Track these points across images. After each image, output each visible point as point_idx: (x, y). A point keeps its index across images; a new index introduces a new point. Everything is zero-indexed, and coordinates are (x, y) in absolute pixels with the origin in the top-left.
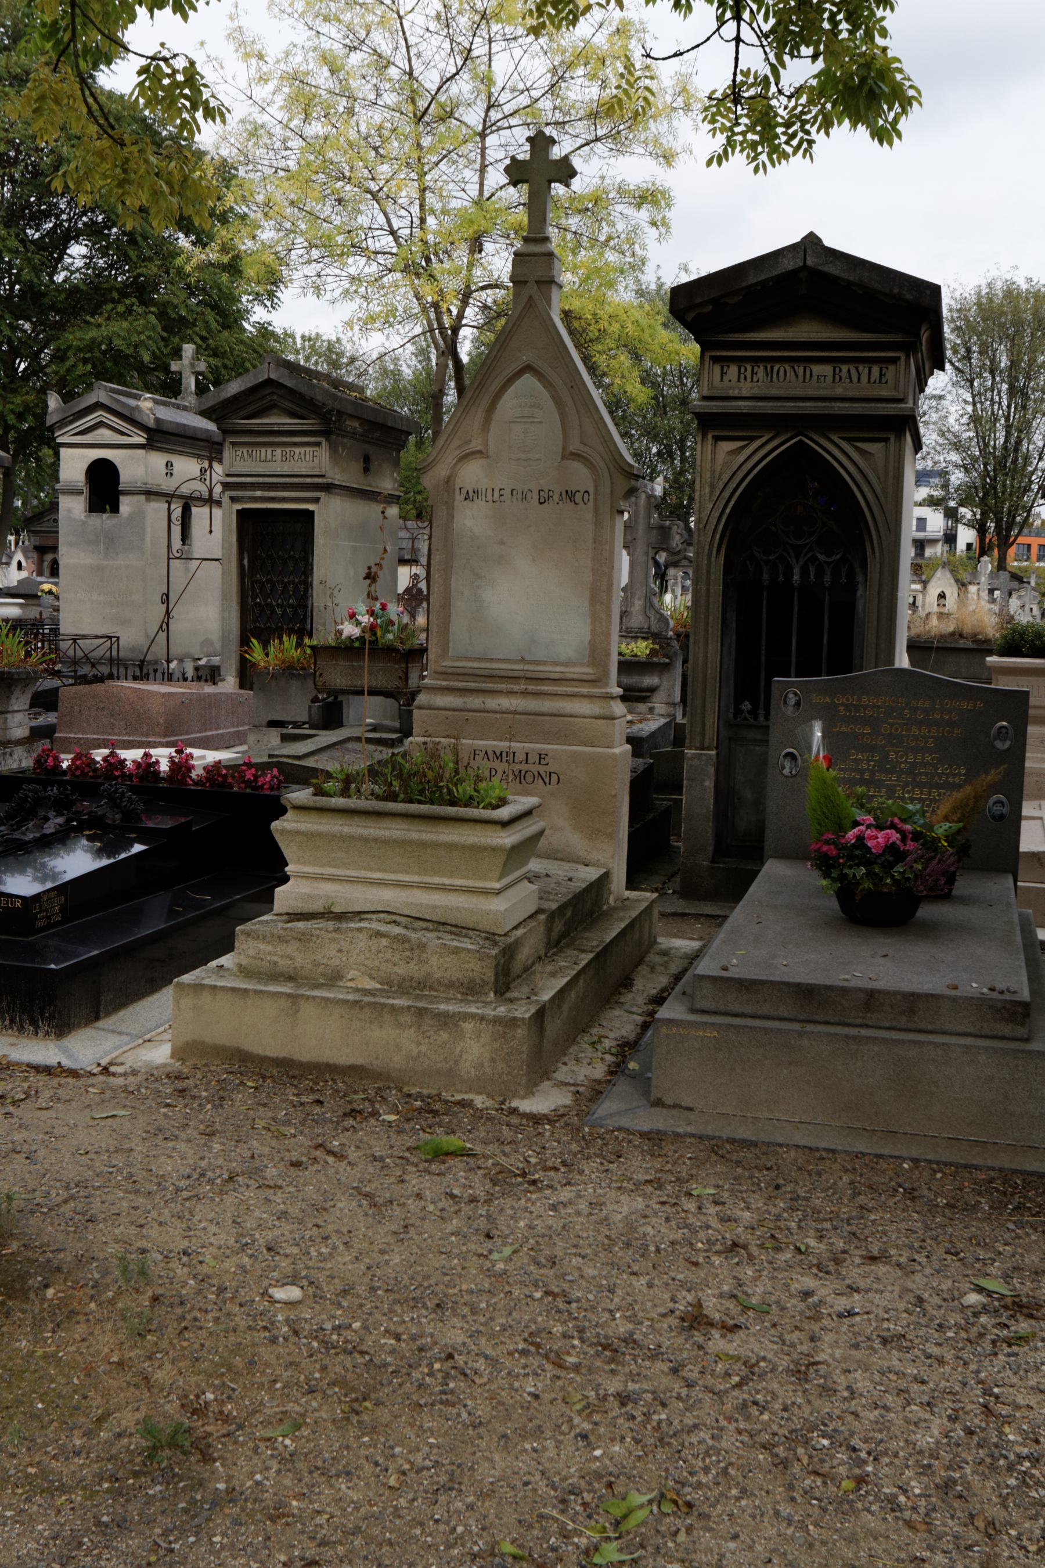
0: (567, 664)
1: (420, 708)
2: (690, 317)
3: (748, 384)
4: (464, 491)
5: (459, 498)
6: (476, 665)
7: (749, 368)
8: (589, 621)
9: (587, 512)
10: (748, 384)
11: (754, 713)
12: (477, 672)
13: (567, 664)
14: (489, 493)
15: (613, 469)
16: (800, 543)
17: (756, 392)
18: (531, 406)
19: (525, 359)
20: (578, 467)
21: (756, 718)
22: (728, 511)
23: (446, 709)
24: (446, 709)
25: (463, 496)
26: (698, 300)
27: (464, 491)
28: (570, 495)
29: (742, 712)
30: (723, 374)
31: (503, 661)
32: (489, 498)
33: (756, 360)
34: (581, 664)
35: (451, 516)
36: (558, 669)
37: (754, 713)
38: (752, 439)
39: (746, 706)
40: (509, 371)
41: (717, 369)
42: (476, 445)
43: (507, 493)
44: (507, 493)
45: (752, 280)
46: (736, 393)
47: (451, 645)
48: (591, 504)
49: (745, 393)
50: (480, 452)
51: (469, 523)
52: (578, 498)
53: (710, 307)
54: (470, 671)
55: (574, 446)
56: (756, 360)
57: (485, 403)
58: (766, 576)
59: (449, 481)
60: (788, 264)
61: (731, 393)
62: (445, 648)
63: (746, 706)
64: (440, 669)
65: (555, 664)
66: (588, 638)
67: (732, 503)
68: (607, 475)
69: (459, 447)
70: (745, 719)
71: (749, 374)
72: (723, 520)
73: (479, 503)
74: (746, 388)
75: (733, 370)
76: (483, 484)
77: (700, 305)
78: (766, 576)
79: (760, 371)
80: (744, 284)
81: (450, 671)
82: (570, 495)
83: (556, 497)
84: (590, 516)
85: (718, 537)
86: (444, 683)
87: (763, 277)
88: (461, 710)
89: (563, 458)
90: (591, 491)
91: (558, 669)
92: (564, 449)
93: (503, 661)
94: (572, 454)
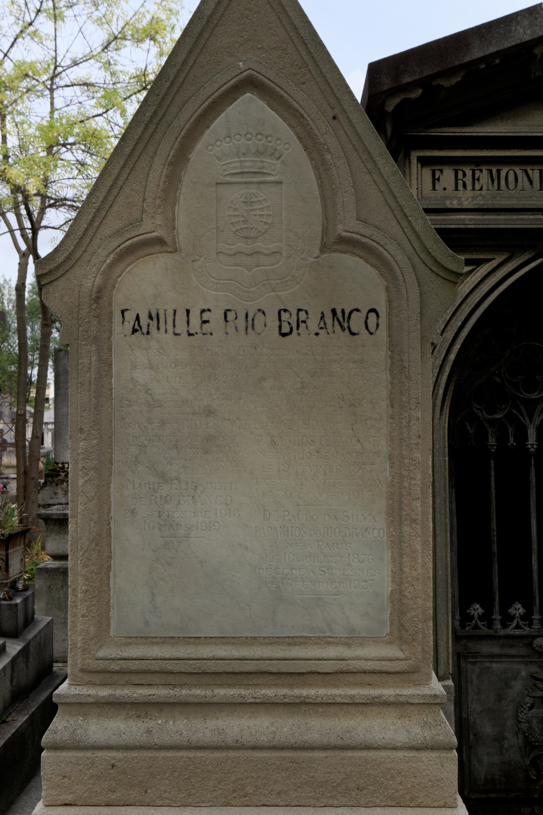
0: (351, 640)
1: (55, 747)
2: (508, 19)
3: (469, 193)
4: (130, 317)
5: (120, 330)
6: (166, 652)
7: (469, 173)
8: (387, 555)
9: (376, 348)
10: (469, 193)
11: (487, 618)
12: (170, 666)
13: (348, 642)
14: (181, 317)
15: (421, 267)
16: (533, 396)
17: (480, 203)
18: (259, 153)
19: (243, 65)
20: (351, 263)
21: (490, 625)
22: (452, 357)
23: (110, 748)
24: (110, 748)
25: (129, 326)
26: (407, 79)
27: (130, 317)
28: (341, 318)
29: (472, 617)
30: (435, 180)
31: (222, 640)
32: (181, 327)
33: (478, 162)
34: (377, 641)
35: (106, 365)
36: (332, 652)
37: (487, 618)
38: (478, 263)
39: (477, 610)
40: (212, 88)
41: (427, 173)
42: (152, 227)
43: (216, 317)
44: (216, 317)
45: (476, 53)
46: (455, 204)
47: (113, 614)
48: (382, 334)
49: (466, 204)
50: (160, 241)
51: (142, 376)
52: (357, 322)
53: (420, 91)
54: (155, 666)
55: (348, 225)
56: (478, 162)
57: (167, 148)
58: (492, 441)
59: (100, 296)
60: (523, 34)
61: (448, 204)
62: (103, 622)
63: (477, 610)
64: (95, 665)
65: (325, 641)
66: (388, 588)
67: (457, 346)
68: (411, 278)
69: (119, 232)
70: (476, 627)
71: (468, 180)
72: (447, 369)
73: (162, 337)
74: (467, 198)
75: (447, 176)
76: (170, 301)
77: (406, 88)
78: (492, 441)
79: (484, 176)
80: (467, 59)
81: (115, 666)
82: (341, 318)
83: (313, 323)
84: (381, 355)
85: (441, 391)
86: (104, 692)
87: (492, 49)
88: (141, 748)
89: (324, 248)
90: (382, 310)
91: (332, 652)
92: (325, 232)
93: (222, 640)
94: (342, 240)
